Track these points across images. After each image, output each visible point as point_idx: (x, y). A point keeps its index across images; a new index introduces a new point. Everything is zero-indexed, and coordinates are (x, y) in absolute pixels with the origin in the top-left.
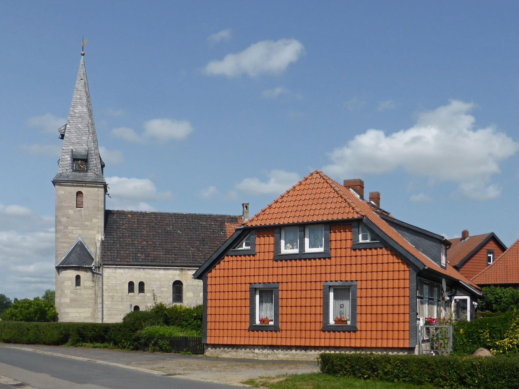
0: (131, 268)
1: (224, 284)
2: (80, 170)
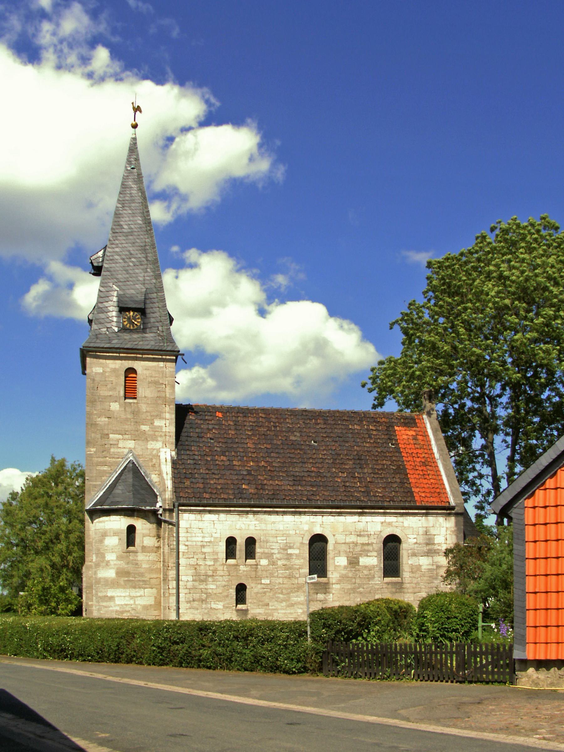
0: (230, 511)
1: (545, 524)
2: (132, 328)
